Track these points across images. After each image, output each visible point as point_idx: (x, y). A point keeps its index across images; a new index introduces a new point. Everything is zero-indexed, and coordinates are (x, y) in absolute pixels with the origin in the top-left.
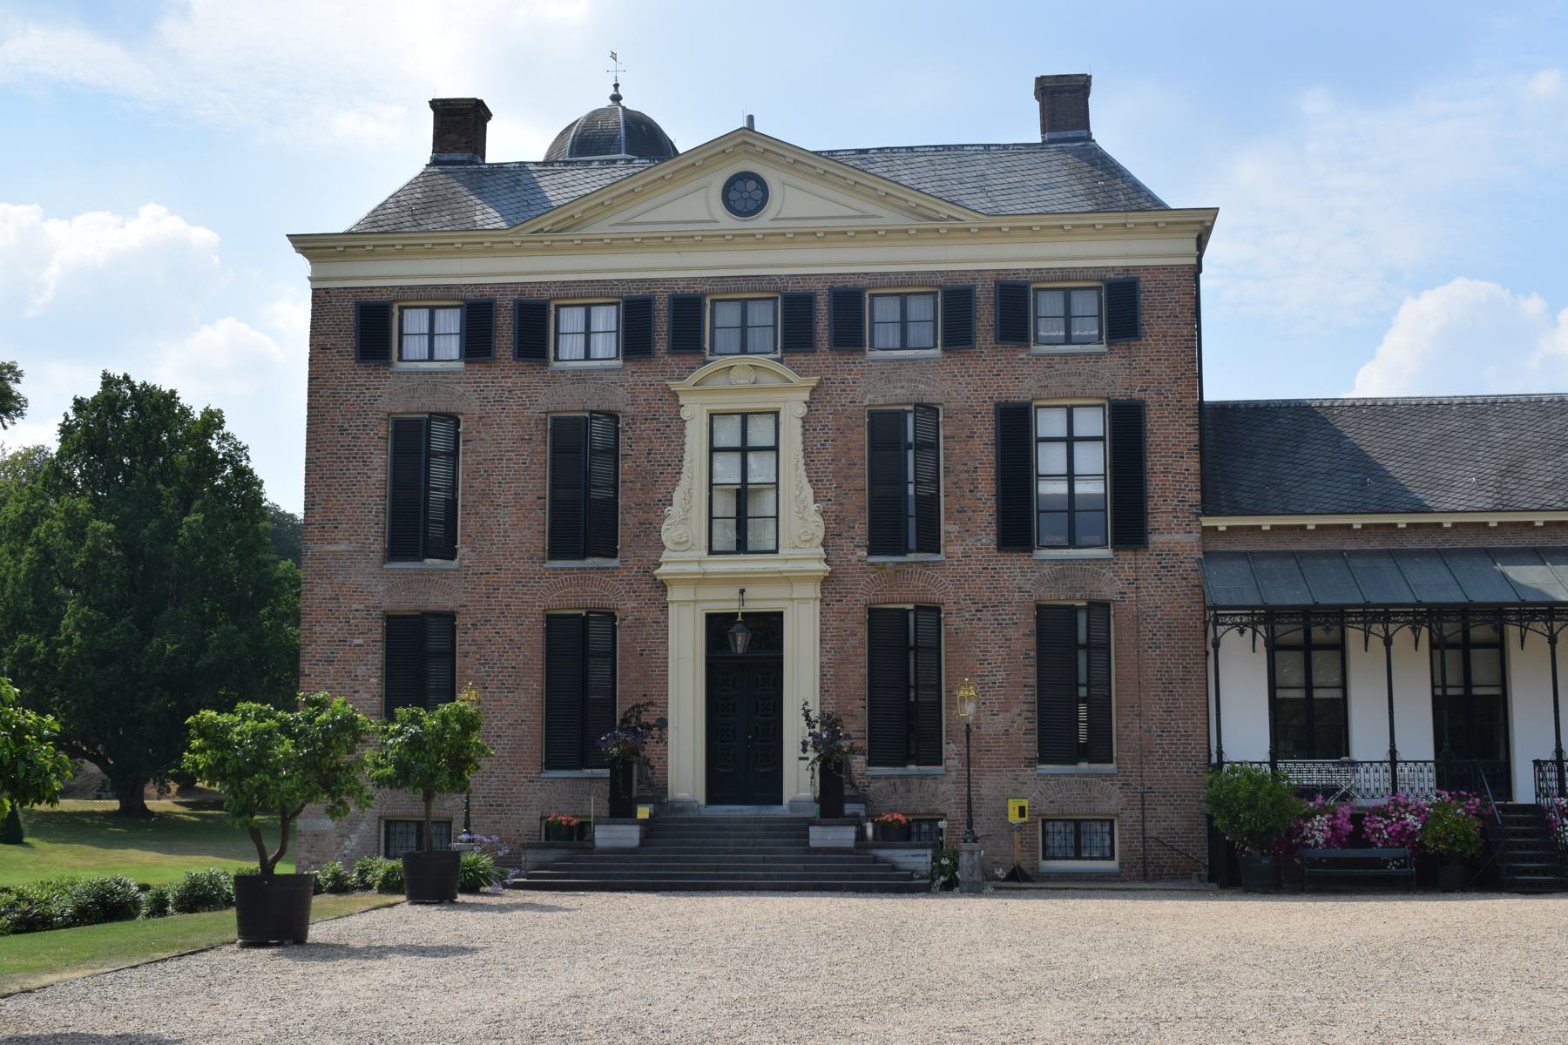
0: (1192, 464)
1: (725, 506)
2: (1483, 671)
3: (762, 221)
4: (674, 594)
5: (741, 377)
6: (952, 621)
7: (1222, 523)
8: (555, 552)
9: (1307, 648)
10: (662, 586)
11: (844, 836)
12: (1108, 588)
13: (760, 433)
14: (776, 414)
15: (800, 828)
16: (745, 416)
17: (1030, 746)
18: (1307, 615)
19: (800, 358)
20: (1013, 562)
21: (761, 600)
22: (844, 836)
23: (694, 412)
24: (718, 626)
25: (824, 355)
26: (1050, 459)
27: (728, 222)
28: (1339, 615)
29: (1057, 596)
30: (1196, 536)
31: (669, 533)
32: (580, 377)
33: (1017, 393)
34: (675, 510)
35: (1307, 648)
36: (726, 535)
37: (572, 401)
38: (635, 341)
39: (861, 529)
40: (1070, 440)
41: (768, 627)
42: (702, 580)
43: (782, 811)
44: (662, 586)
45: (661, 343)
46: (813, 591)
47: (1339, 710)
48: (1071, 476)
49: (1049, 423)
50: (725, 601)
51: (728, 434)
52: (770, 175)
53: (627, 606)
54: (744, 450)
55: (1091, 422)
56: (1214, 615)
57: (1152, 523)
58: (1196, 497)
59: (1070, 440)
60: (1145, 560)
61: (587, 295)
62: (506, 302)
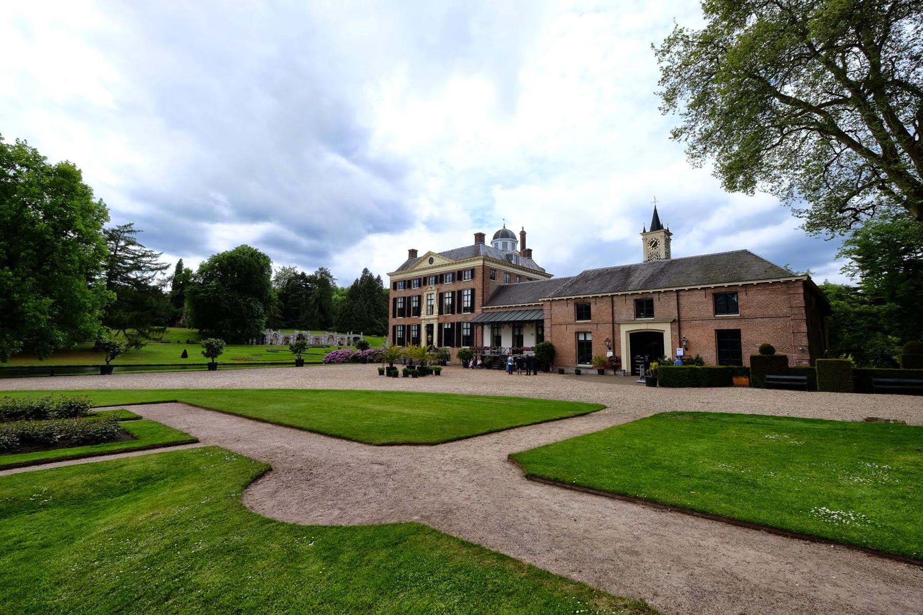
1: (429, 307)
3: (433, 265)
7: (484, 308)
21: (431, 322)
23: (425, 294)
27: (430, 265)
30: (481, 310)
36: (429, 313)
40: (468, 295)
42: (425, 319)
46: (436, 320)
49: (466, 293)
52: (434, 258)
54: (431, 300)
58: (481, 303)
59: (468, 295)
60: (475, 314)
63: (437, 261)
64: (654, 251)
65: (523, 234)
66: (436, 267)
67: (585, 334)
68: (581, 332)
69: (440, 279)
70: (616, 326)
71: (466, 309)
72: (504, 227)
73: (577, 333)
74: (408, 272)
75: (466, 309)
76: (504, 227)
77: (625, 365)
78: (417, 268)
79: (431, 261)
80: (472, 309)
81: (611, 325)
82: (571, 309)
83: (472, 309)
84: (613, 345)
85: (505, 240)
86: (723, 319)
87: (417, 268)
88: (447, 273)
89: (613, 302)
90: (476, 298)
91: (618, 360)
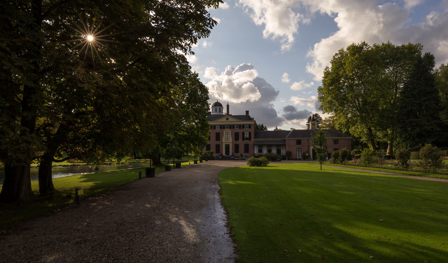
0: (254, 136)
2: (270, 148)
3: (228, 121)
6: (239, 145)
8: (216, 141)
11: (233, 157)
12: (249, 143)
13: (228, 134)
15: (230, 157)
18: (260, 145)
19: (231, 129)
20: (243, 141)
21: (228, 144)
22: (233, 157)
23: (224, 132)
24: (226, 145)
26: (245, 135)
27: (227, 121)
28: (262, 145)
29: (246, 143)
31: (223, 139)
33: (243, 131)
34: (223, 138)
36: (226, 140)
37: (217, 132)
40: (247, 134)
41: (229, 145)
45: (222, 128)
49: (245, 133)
50: (226, 144)
51: (226, 133)
55: (248, 133)
56: (254, 145)
57: (251, 139)
59: (247, 134)
61: (218, 125)
64: (313, 126)
65: (228, 106)
66: (231, 122)
67: (299, 149)
69: (231, 127)
71: (247, 139)
73: (297, 149)
75: (247, 139)
77: (312, 157)
78: (219, 121)
79: (227, 119)
80: (249, 139)
82: (295, 142)
83: (249, 139)
84: (308, 152)
85: (220, 107)
87: (219, 121)
90: (251, 135)
91: (310, 156)
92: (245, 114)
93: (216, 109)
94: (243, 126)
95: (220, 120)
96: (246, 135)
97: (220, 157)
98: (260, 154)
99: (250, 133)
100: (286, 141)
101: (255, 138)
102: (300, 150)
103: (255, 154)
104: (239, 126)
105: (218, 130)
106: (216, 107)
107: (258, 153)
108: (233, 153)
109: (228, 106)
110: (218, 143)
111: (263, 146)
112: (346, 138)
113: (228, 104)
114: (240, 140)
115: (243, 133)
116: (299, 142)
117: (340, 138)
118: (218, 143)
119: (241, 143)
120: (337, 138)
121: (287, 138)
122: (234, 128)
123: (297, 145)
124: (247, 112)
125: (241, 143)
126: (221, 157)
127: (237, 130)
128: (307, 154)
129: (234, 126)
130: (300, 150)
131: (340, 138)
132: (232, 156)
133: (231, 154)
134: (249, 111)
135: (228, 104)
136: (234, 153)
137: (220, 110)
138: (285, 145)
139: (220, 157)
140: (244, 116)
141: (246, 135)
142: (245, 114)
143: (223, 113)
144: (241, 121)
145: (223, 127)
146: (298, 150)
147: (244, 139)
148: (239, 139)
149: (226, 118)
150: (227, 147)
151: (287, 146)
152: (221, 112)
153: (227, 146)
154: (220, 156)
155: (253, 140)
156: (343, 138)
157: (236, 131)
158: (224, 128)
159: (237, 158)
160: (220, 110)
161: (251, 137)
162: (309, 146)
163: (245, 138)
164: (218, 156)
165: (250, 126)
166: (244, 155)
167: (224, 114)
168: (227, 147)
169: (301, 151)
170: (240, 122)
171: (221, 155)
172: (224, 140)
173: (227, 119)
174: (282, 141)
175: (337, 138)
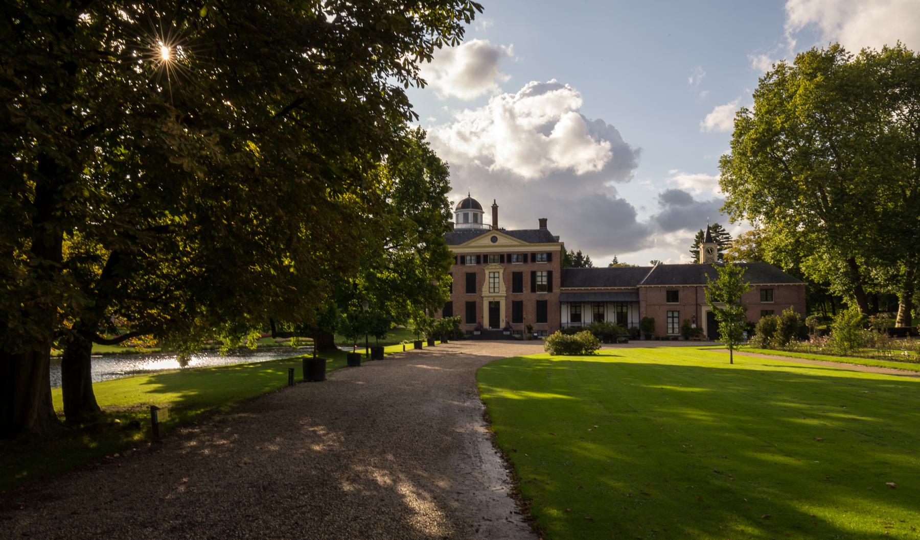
0: (559, 280)
3: (496, 244)
4: (484, 299)
5: (494, 267)
6: (524, 303)
7: (563, 289)
8: (467, 292)
9: (576, 307)
10: (482, 297)
11: (508, 333)
12: (547, 298)
13: (497, 275)
14: (499, 272)
15: (502, 332)
16: (494, 273)
17: (536, 320)
18: (576, 303)
19: (502, 264)
20: (533, 294)
21: (497, 299)
22: (508, 333)
23: (487, 272)
24: (490, 303)
25: (506, 264)
26: (539, 279)
27: (492, 244)
28: (580, 302)
29: (540, 299)
31: (484, 290)
32: (470, 267)
34: (484, 286)
35: (576, 307)
36: (492, 290)
37: (470, 271)
38: (478, 262)
39: (511, 289)
40: (542, 276)
41: (498, 303)
42: (488, 297)
43: (500, 329)
44: (482, 297)
45: (482, 261)
46: (504, 298)
47: (580, 315)
48: (542, 282)
49: (539, 274)
50: (491, 300)
51: (492, 275)
53: (477, 300)
55: (545, 274)
56: (561, 303)
59: (542, 276)
60: (552, 294)
61: (471, 254)
62: (459, 256)
63: (502, 240)
68: (676, 311)
70: (698, 307)
71: (542, 288)
72: (469, 195)
74: (463, 248)
75: (542, 288)
76: (469, 195)
77: (705, 333)
78: (473, 244)
79: (494, 239)
80: (549, 288)
81: (695, 306)
82: (664, 294)
83: (549, 288)
84: (697, 319)
85: (476, 211)
86: (764, 304)
87: (473, 244)
88: (518, 254)
89: (696, 290)
90: (554, 279)
91: (701, 329)
92: (537, 227)
93: (466, 216)
94: (534, 256)
95: (477, 242)
96: (542, 280)
97: (476, 333)
98: (576, 324)
99: (550, 275)
100: (641, 293)
101: (562, 285)
102: (676, 314)
103: (563, 325)
104: (525, 258)
105: (471, 266)
106: (466, 211)
107: (569, 321)
108: (507, 323)
109: (495, 209)
110: (471, 297)
111: (582, 305)
112: (791, 284)
113: (495, 204)
114: (524, 292)
115: (533, 274)
116: (673, 296)
117: (776, 284)
118: (471, 297)
119: (529, 298)
120: (769, 284)
121: (643, 284)
122: (509, 261)
123: (668, 302)
124: (543, 222)
125: (529, 298)
126: (479, 333)
127: (517, 266)
128: (693, 326)
129: (509, 256)
130: (676, 314)
131: (776, 284)
132: (506, 329)
133: (503, 325)
134: (546, 220)
135: (495, 204)
136: (511, 323)
137: (475, 216)
138: (638, 302)
139: (476, 333)
140: (535, 231)
141: (542, 280)
142: (537, 227)
143: (482, 224)
144: (527, 244)
145: (483, 259)
146: (670, 314)
147: (534, 287)
148: (524, 289)
149: (490, 237)
150: (494, 308)
151: (643, 304)
152: (479, 222)
153: (493, 306)
154: (477, 330)
155: (557, 290)
156: (784, 284)
157: (517, 270)
158: (486, 261)
159: (517, 336)
160: (475, 216)
161: (554, 283)
162: (698, 306)
163: (538, 285)
164: (472, 329)
165: (549, 256)
166: (536, 326)
167: (484, 227)
168: (494, 308)
169: (678, 317)
170: (526, 246)
171: (480, 328)
172: (485, 291)
173: (494, 239)
174: (631, 293)
175: (769, 284)
